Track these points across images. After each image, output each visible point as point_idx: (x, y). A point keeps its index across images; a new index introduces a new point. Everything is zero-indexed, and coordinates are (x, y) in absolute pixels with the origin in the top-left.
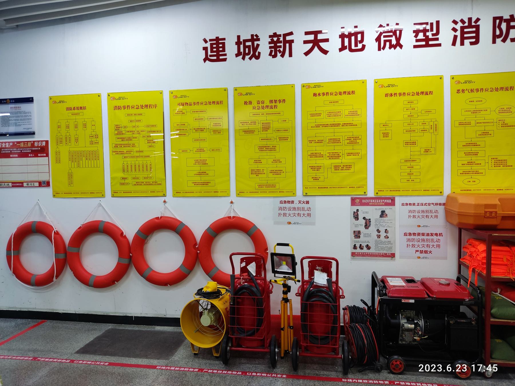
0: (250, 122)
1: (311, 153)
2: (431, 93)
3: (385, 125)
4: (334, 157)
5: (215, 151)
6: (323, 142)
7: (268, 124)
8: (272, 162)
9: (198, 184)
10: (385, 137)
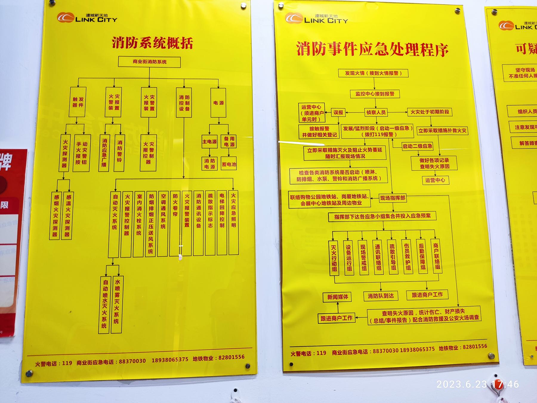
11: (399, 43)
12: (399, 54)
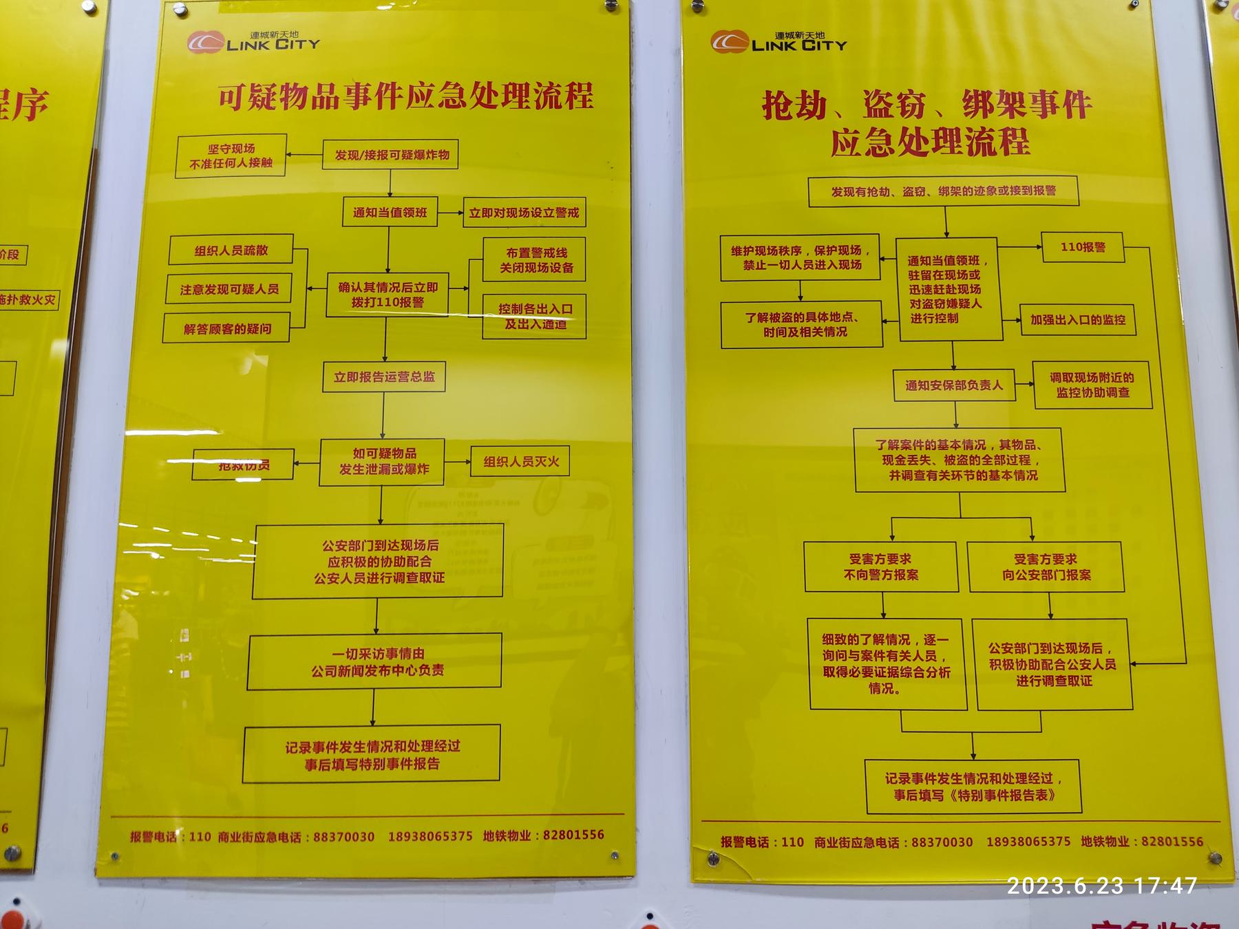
0: (808, 246)
5: (515, 470)
7: (957, 268)
8: (1008, 574)
9: (339, 765)
11: (489, 84)
12: (489, 106)
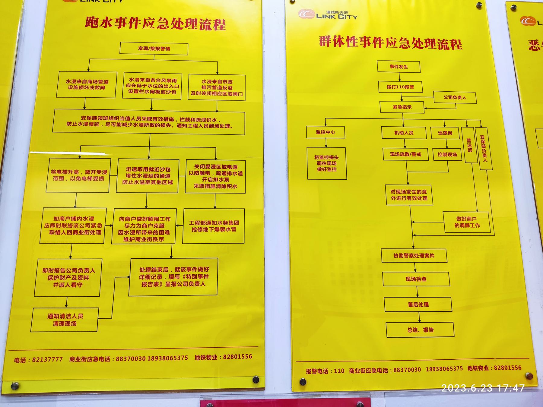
1: (56, 218)
2: (456, 44)
3: (323, 132)
4: (141, 236)
6: (106, 177)
10: (324, 169)
